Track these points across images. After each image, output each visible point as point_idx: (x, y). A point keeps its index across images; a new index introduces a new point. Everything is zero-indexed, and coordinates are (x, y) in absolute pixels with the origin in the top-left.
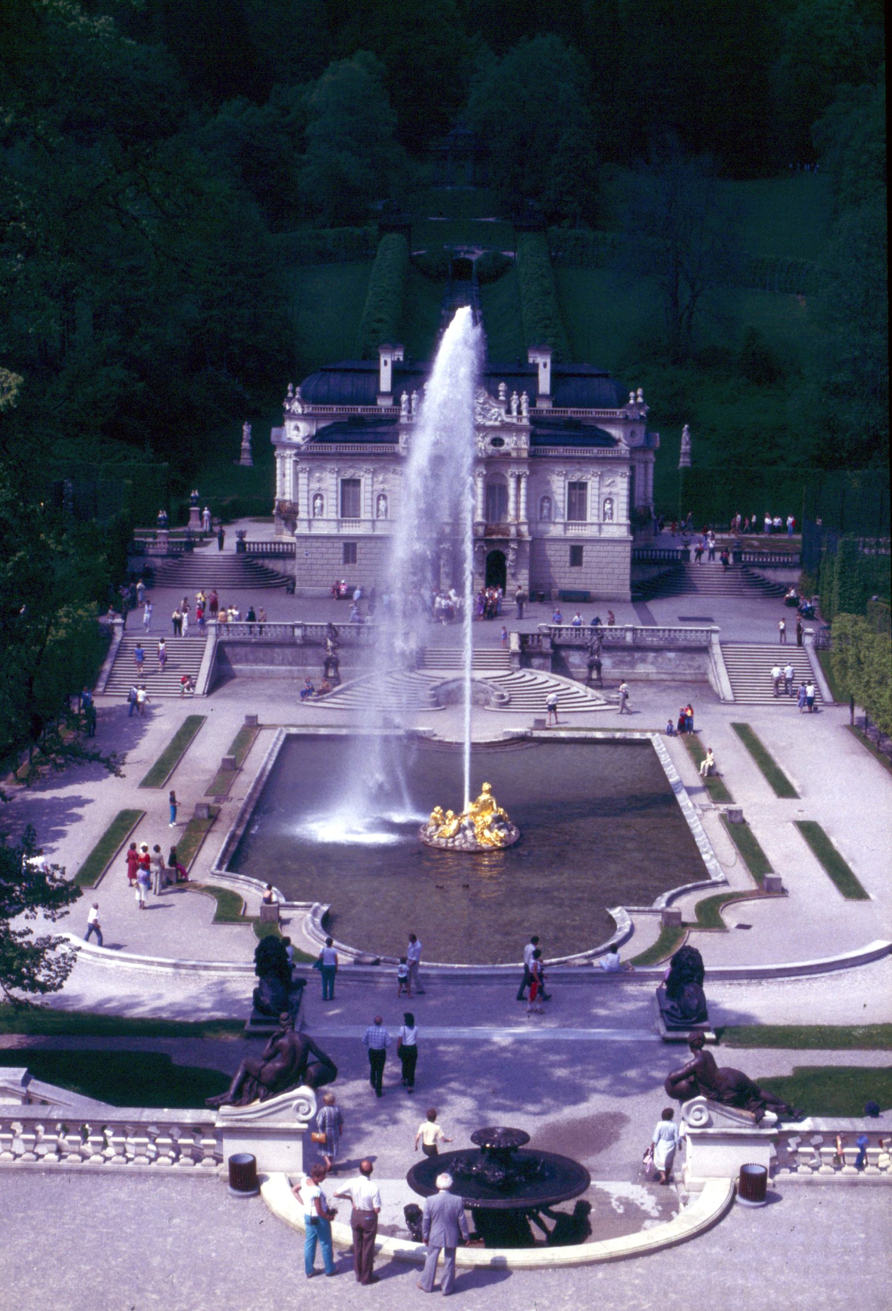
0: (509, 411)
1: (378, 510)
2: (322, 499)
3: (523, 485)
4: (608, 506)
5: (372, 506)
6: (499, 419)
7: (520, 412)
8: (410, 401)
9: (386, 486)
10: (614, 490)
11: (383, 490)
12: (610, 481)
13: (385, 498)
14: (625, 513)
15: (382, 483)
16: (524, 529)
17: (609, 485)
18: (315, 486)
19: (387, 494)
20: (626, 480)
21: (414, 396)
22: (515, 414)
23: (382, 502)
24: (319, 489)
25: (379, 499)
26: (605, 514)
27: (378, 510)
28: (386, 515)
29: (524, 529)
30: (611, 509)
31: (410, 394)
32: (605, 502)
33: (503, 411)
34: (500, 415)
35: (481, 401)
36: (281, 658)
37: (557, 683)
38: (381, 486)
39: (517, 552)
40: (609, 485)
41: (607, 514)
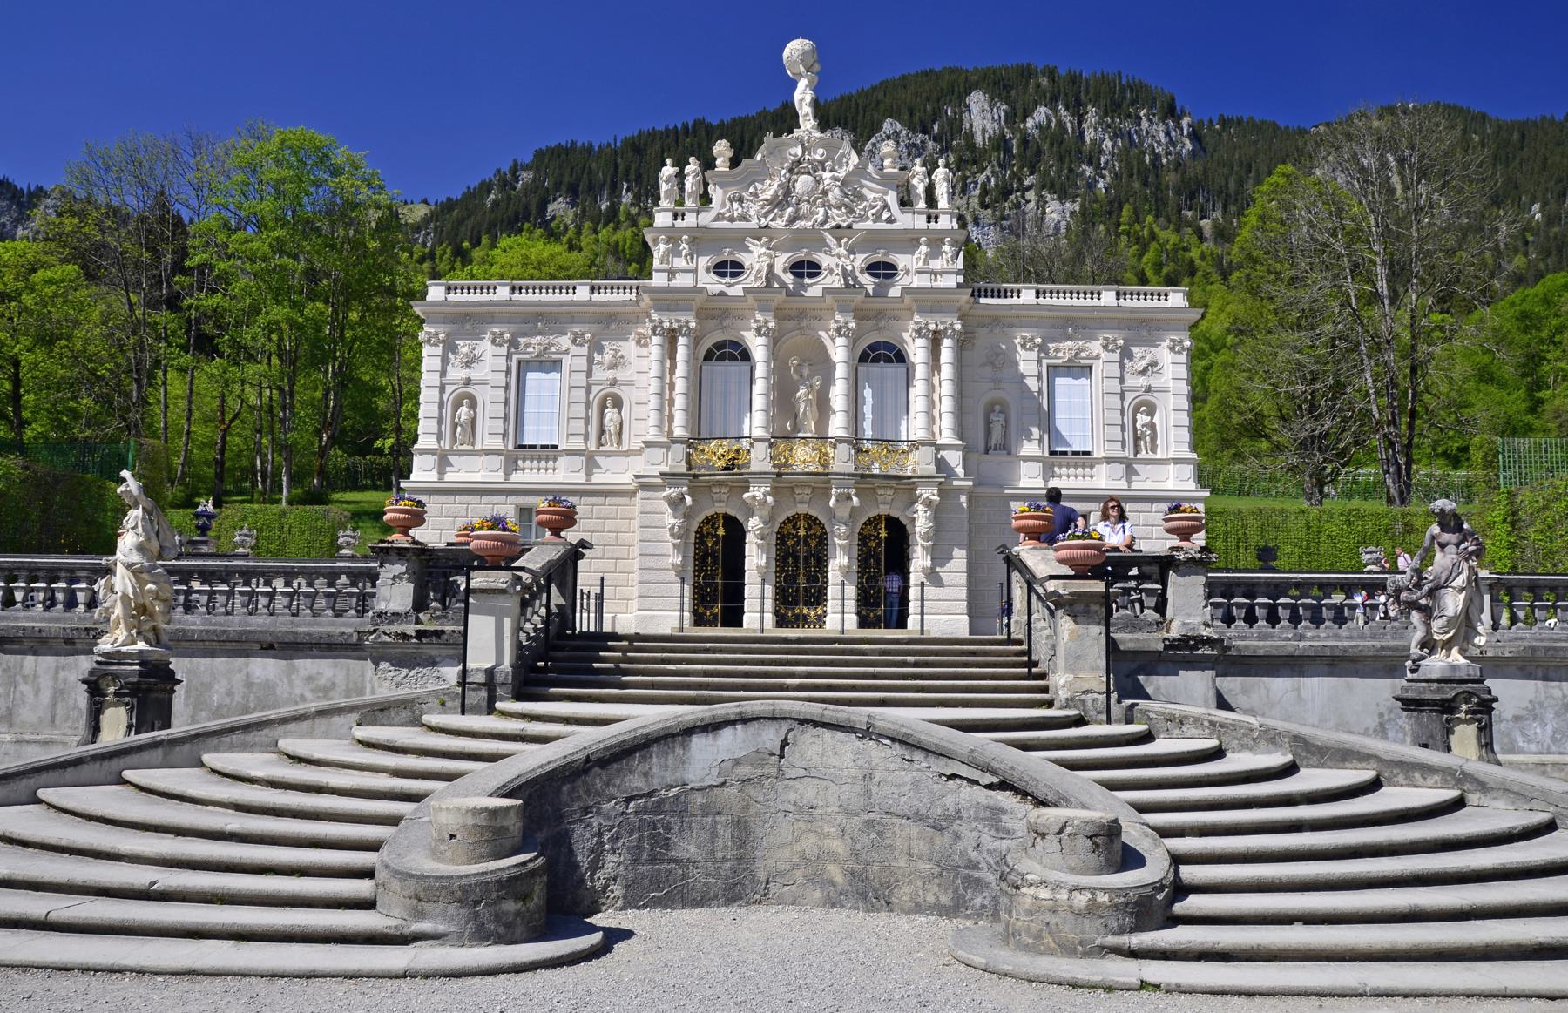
0: (906, 203)
1: (602, 432)
2: (473, 404)
3: (946, 354)
4: (1142, 419)
5: (587, 421)
6: (885, 216)
7: (931, 201)
8: (681, 176)
9: (620, 374)
10: (1155, 382)
11: (614, 382)
12: (1144, 363)
13: (618, 403)
14: (1185, 435)
15: (612, 366)
16: (954, 459)
17: (1143, 372)
18: (456, 373)
19: (623, 392)
20: (1183, 358)
21: (692, 167)
22: (922, 205)
23: (610, 413)
24: (468, 382)
25: (603, 407)
26: (1137, 439)
27: (602, 432)
28: (619, 443)
29: (954, 459)
30: (1152, 426)
31: (681, 163)
32: (1136, 410)
33: (892, 198)
34: (886, 206)
35: (842, 173)
36: (46, 696)
37: (1365, 775)
38: (609, 374)
39: (938, 514)
40: (1143, 372)
41: (1142, 439)
